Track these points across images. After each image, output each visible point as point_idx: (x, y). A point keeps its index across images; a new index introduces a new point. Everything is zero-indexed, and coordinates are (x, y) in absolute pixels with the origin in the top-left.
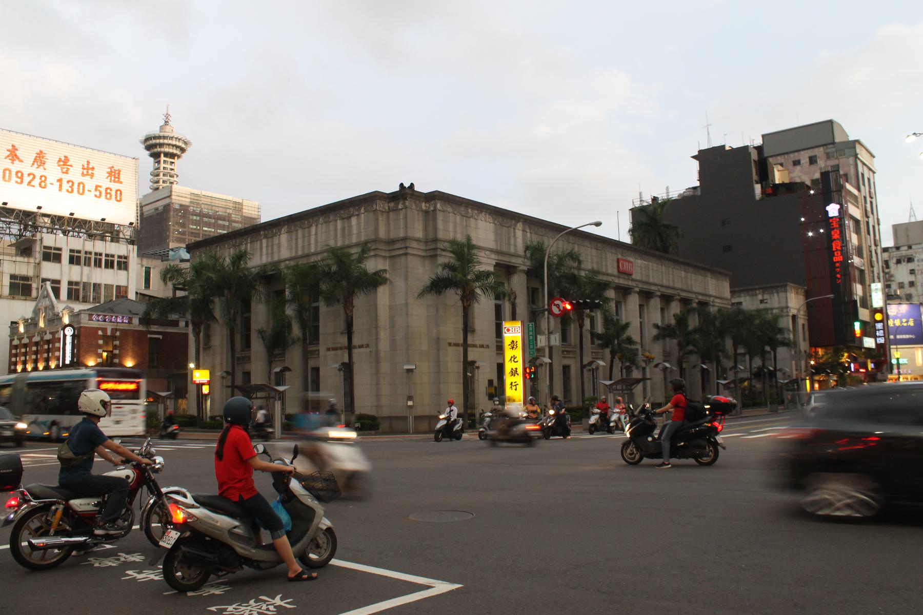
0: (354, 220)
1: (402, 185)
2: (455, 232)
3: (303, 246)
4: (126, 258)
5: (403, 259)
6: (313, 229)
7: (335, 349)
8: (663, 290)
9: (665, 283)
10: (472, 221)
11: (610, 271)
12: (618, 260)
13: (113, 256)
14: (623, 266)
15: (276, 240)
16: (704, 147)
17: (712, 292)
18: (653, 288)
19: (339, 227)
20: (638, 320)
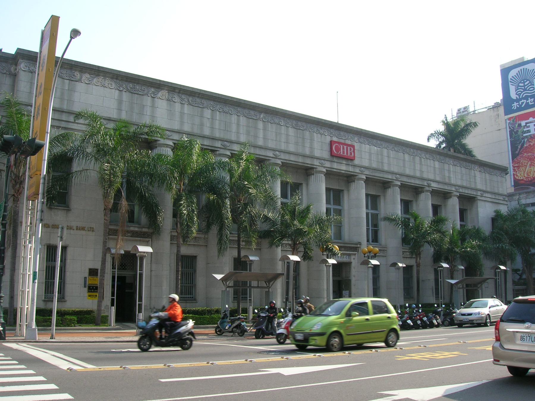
8: (405, 179)
9: (408, 172)
11: (317, 153)
12: (331, 143)
14: (338, 149)
17: (479, 186)
18: (390, 176)
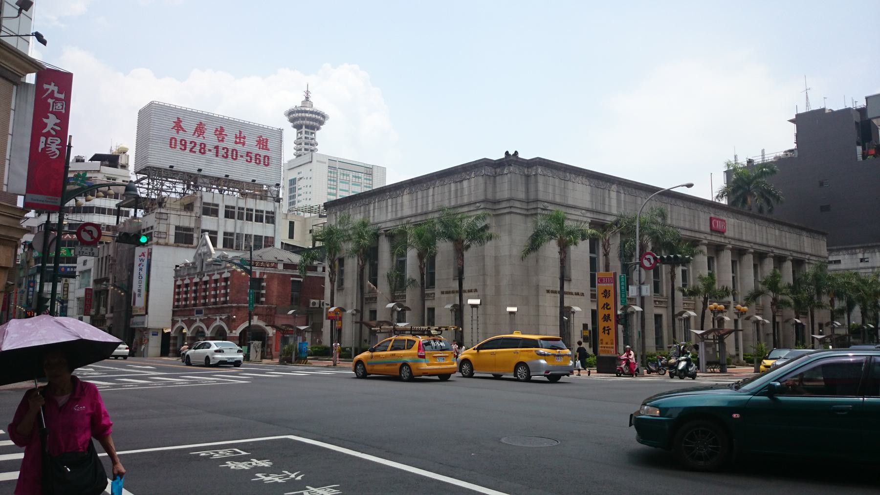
0: (465, 183)
1: (507, 153)
2: (554, 194)
3: (422, 205)
4: (273, 213)
5: (507, 217)
6: (431, 191)
7: (448, 293)
8: (756, 247)
9: (758, 240)
10: (570, 184)
11: (702, 229)
12: (711, 219)
13: (262, 211)
14: (715, 224)
15: (399, 200)
16: (802, 110)
17: (807, 250)
18: (746, 245)
19: (453, 189)
20: (731, 275)
